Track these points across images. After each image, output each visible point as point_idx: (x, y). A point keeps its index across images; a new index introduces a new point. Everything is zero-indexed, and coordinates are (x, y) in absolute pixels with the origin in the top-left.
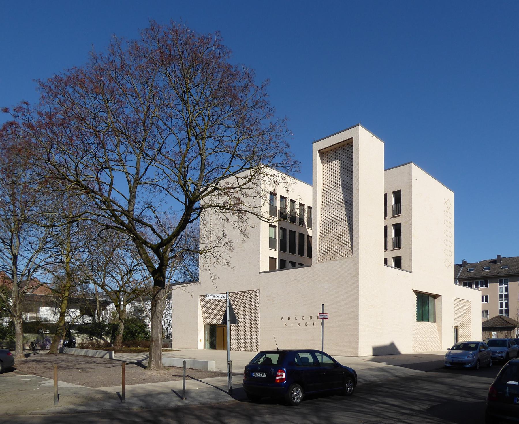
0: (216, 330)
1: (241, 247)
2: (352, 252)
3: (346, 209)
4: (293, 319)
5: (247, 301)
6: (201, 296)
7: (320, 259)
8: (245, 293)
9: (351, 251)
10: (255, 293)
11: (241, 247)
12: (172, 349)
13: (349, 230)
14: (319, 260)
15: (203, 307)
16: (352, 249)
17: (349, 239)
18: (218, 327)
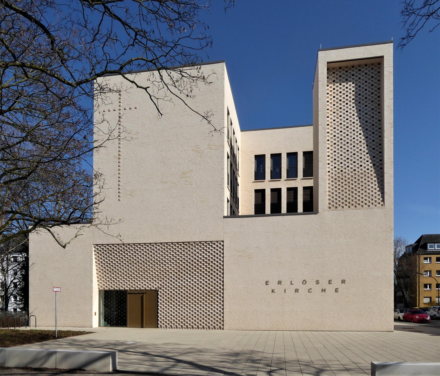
0: (126, 298)
1: (186, 177)
2: (383, 201)
3: (367, 146)
4: (286, 284)
5: (196, 257)
6: (97, 245)
7: (331, 206)
8: (194, 245)
9: (381, 199)
10: (214, 246)
11: (186, 177)
12: (32, 327)
13: (375, 173)
14: (330, 208)
15: (100, 262)
16: (383, 197)
17: (375, 185)
18: (129, 293)
